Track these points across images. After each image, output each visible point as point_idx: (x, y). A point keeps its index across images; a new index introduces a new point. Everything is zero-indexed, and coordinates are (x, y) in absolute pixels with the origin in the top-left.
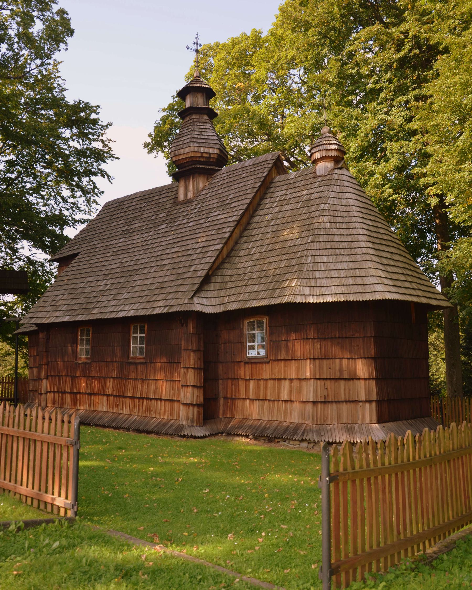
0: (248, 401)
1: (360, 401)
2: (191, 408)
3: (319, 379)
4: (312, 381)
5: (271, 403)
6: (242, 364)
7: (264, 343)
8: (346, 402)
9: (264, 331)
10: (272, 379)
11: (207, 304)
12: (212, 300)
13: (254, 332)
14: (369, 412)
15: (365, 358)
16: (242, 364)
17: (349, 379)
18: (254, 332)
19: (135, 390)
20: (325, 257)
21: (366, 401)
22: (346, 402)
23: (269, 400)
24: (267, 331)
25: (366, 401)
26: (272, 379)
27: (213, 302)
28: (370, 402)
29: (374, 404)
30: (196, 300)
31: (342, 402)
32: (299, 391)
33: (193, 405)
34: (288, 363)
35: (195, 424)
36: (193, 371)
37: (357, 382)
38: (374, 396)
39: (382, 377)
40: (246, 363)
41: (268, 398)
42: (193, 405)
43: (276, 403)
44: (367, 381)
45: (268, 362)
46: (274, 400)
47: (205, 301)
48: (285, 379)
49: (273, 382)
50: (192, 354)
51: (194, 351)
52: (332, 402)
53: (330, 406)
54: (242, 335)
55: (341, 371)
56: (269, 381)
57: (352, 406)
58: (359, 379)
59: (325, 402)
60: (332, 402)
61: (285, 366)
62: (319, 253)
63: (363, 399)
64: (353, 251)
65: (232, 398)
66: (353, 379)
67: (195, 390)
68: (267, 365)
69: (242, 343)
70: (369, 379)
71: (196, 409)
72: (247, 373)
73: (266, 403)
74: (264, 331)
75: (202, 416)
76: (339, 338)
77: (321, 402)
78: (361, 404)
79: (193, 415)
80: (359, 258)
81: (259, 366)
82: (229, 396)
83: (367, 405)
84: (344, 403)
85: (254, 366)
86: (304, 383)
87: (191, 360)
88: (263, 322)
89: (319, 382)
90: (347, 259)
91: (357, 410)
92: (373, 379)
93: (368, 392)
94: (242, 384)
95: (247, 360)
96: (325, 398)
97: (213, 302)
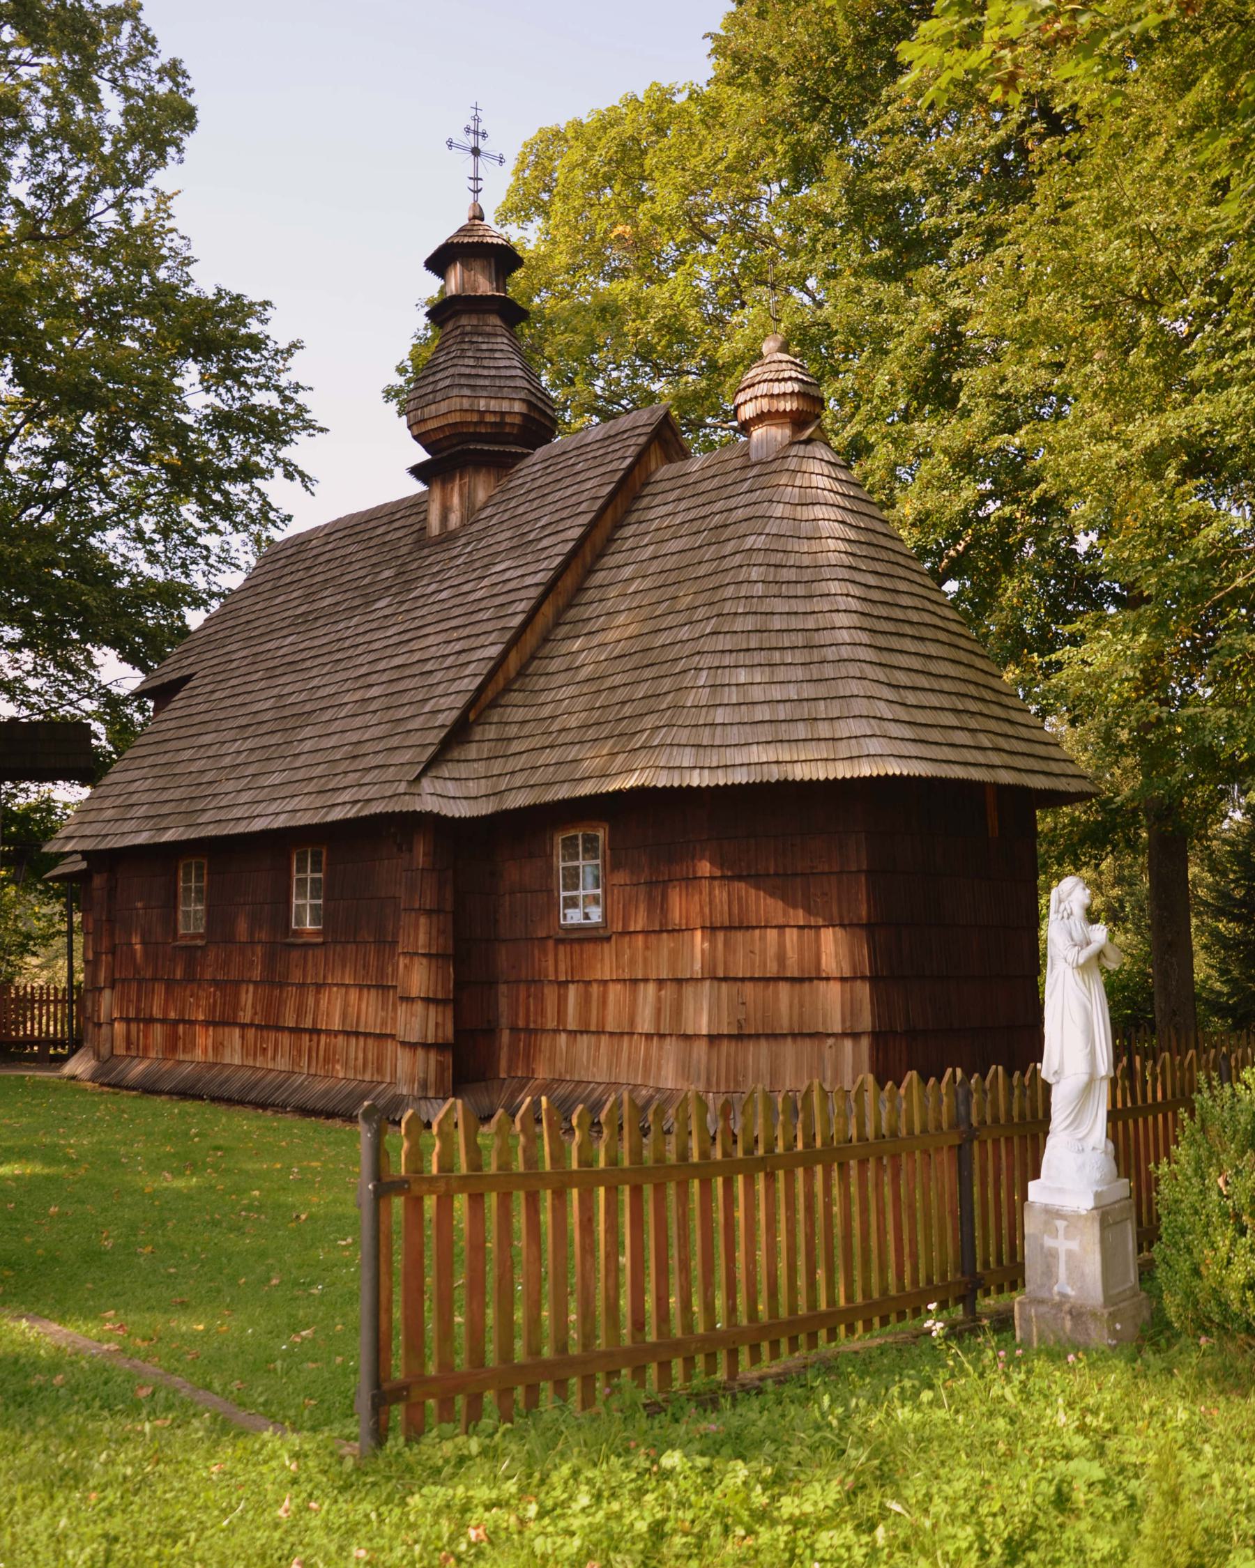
0: (563, 1036)
1: (829, 1035)
2: (420, 1053)
3: (725, 979)
4: (707, 983)
5: (615, 1040)
6: (551, 943)
7: (599, 891)
8: (794, 1036)
9: (599, 862)
10: (618, 981)
11: (454, 796)
12: (471, 783)
13: (575, 863)
14: (852, 1062)
15: (842, 925)
16: (551, 943)
17: (801, 980)
18: (575, 863)
19: (300, 1012)
20: (742, 671)
21: (844, 1035)
22: (794, 1036)
23: (611, 1034)
24: (604, 861)
25: (844, 1035)
26: (618, 981)
27: (473, 788)
28: (855, 1036)
29: (865, 1043)
30: (426, 784)
31: (784, 1036)
32: (678, 1010)
33: (426, 1046)
34: (653, 937)
35: (431, 1094)
36: (424, 961)
37: (822, 985)
38: (866, 1022)
39: (887, 973)
40: (559, 941)
41: (608, 1029)
42: (426, 1046)
43: (626, 1038)
44: (848, 985)
45: (608, 939)
46: (622, 1034)
47: (451, 788)
48: (646, 980)
49: (619, 986)
50: (423, 921)
51: (429, 912)
52: (757, 1036)
53: (751, 1046)
54: (550, 870)
55: (781, 958)
56: (611, 985)
57: (807, 1045)
58: (828, 979)
59: (739, 1037)
60: (757, 1036)
61: (647, 948)
62: (728, 660)
63: (838, 1029)
64: (816, 655)
65: (527, 1030)
66: (810, 979)
67: (432, 1009)
68: (606, 946)
69: (550, 893)
70: (854, 979)
71: (433, 1056)
72: (562, 967)
73: (604, 1039)
74: (599, 862)
75: (449, 1074)
76: (776, 875)
77: (730, 1037)
78: (831, 1041)
79: (426, 1072)
80: (829, 671)
81: (589, 948)
82: (521, 1024)
83: (848, 1044)
84: (789, 1040)
85: (576, 947)
86: (689, 990)
87: (420, 934)
88: (596, 838)
89: (724, 986)
90: (799, 673)
91: (821, 1058)
92: (863, 978)
93: (850, 1010)
94: (551, 994)
95: (561, 935)
96: (740, 1027)
97: (473, 788)
